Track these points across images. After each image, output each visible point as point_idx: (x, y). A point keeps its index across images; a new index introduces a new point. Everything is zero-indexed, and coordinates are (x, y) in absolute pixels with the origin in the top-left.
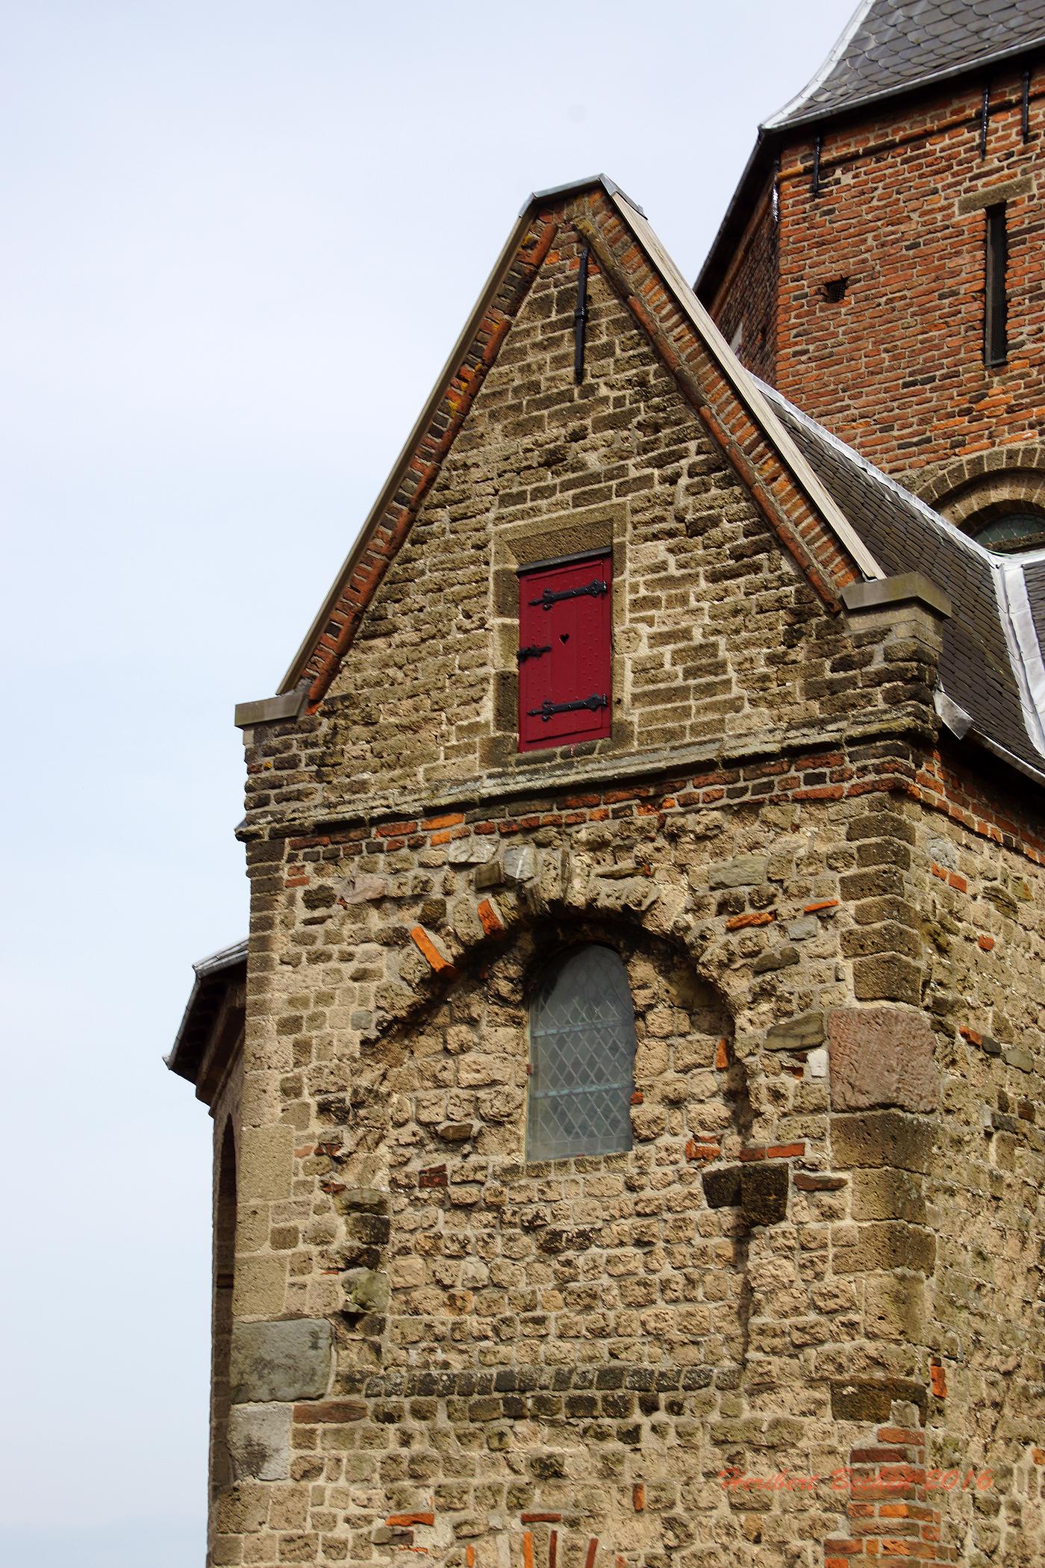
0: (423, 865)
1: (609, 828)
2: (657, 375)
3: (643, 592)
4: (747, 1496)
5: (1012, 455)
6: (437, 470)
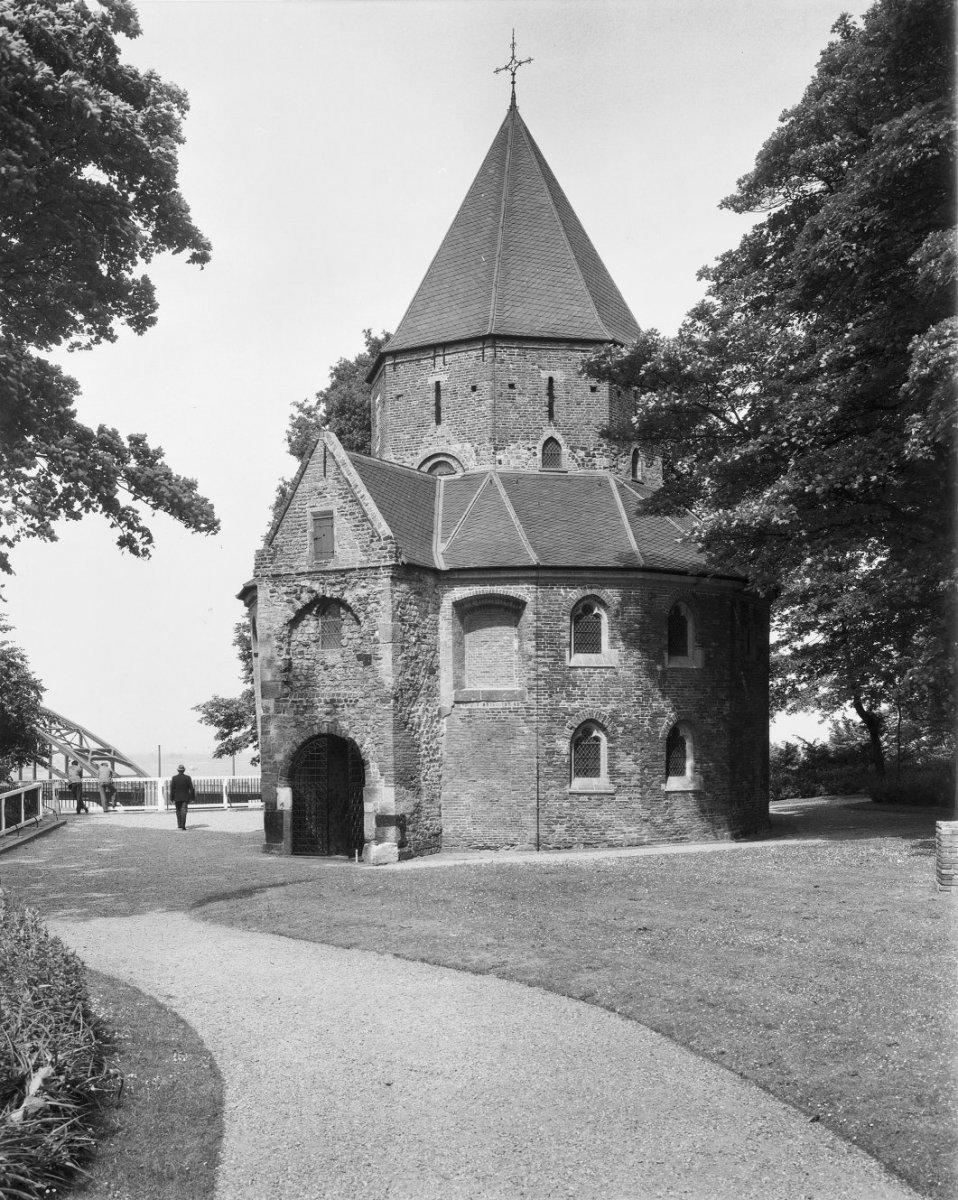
1: (333, 581)
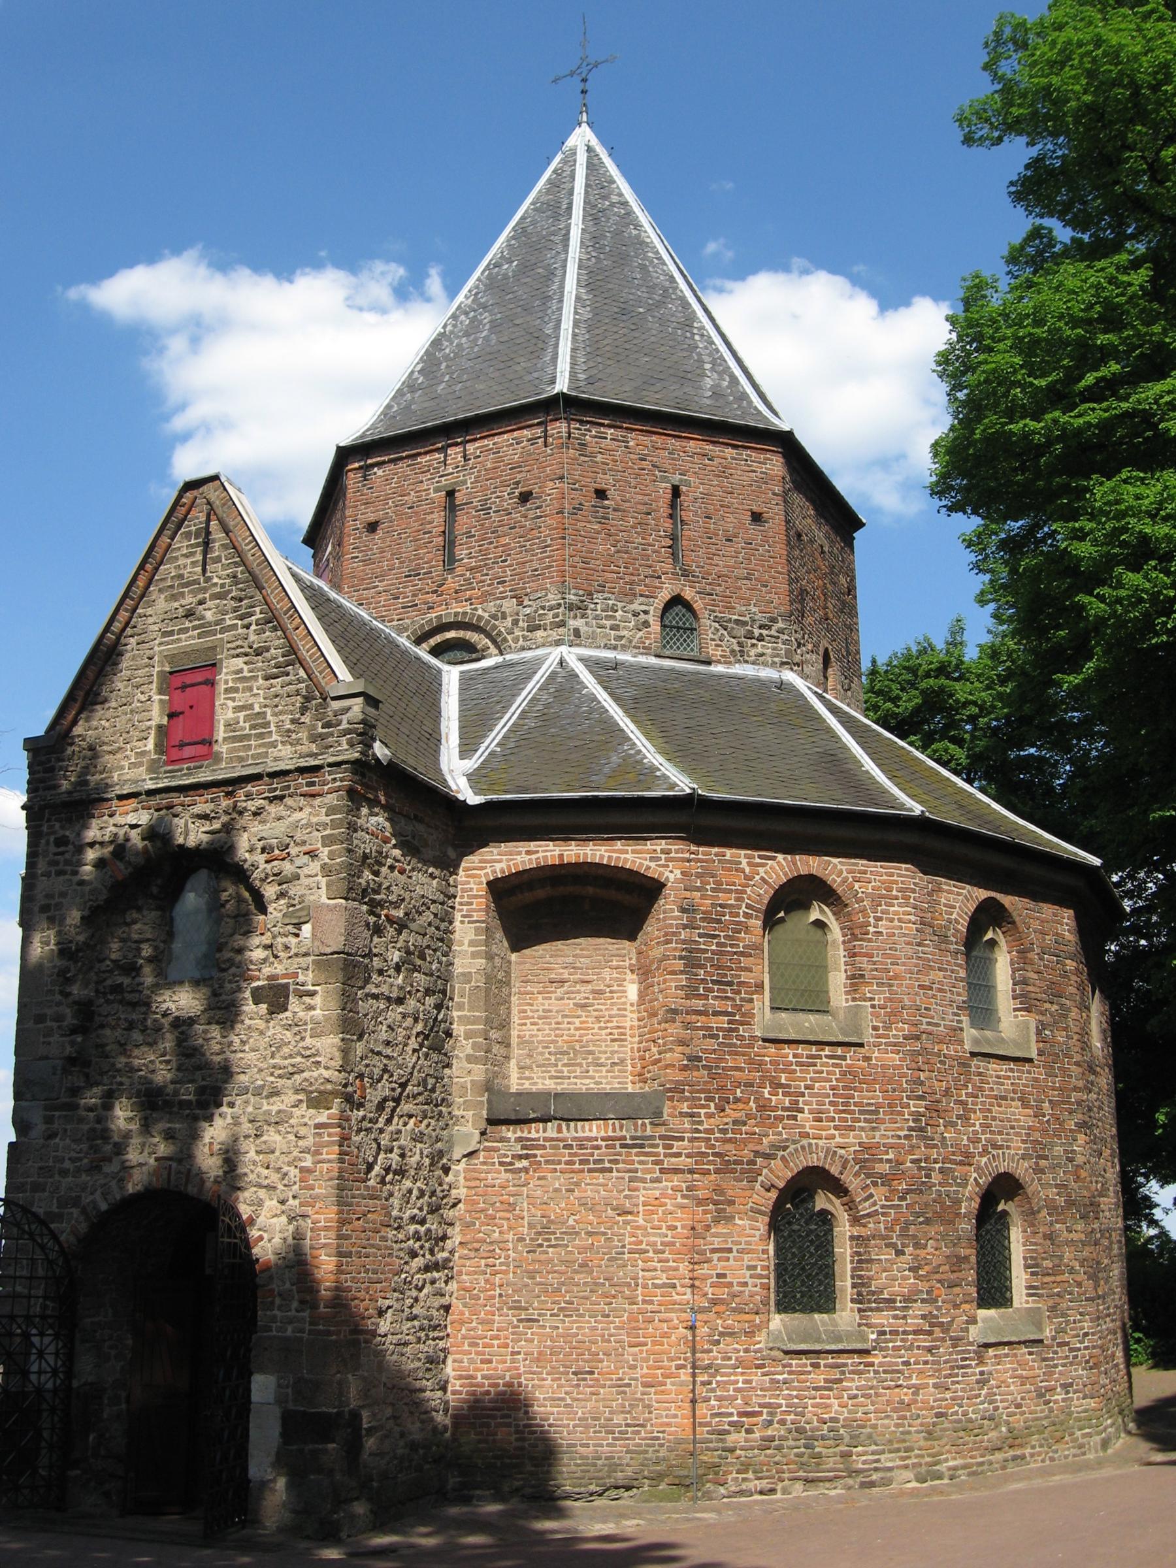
0: (115, 825)
1: (207, 808)
2: (242, 573)
3: (231, 684)
4: (264, 1146)
5: (456, 614)
6: (131, 618)
